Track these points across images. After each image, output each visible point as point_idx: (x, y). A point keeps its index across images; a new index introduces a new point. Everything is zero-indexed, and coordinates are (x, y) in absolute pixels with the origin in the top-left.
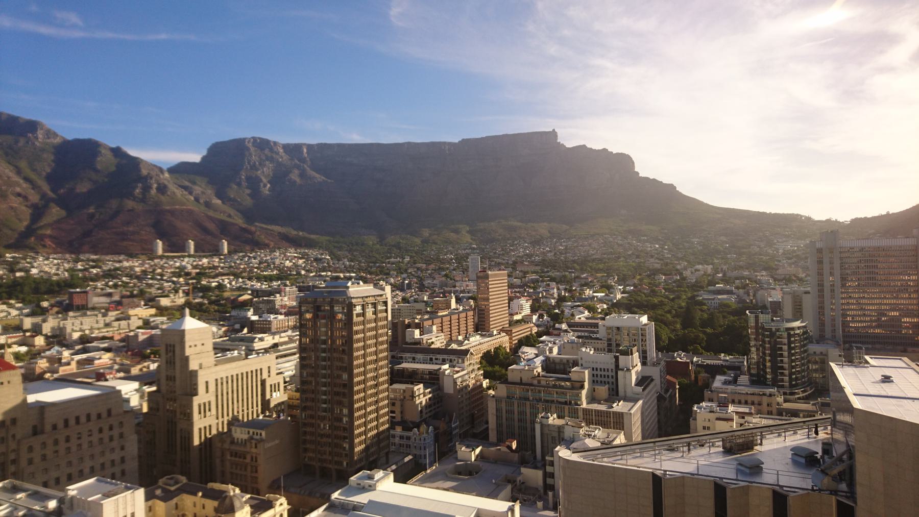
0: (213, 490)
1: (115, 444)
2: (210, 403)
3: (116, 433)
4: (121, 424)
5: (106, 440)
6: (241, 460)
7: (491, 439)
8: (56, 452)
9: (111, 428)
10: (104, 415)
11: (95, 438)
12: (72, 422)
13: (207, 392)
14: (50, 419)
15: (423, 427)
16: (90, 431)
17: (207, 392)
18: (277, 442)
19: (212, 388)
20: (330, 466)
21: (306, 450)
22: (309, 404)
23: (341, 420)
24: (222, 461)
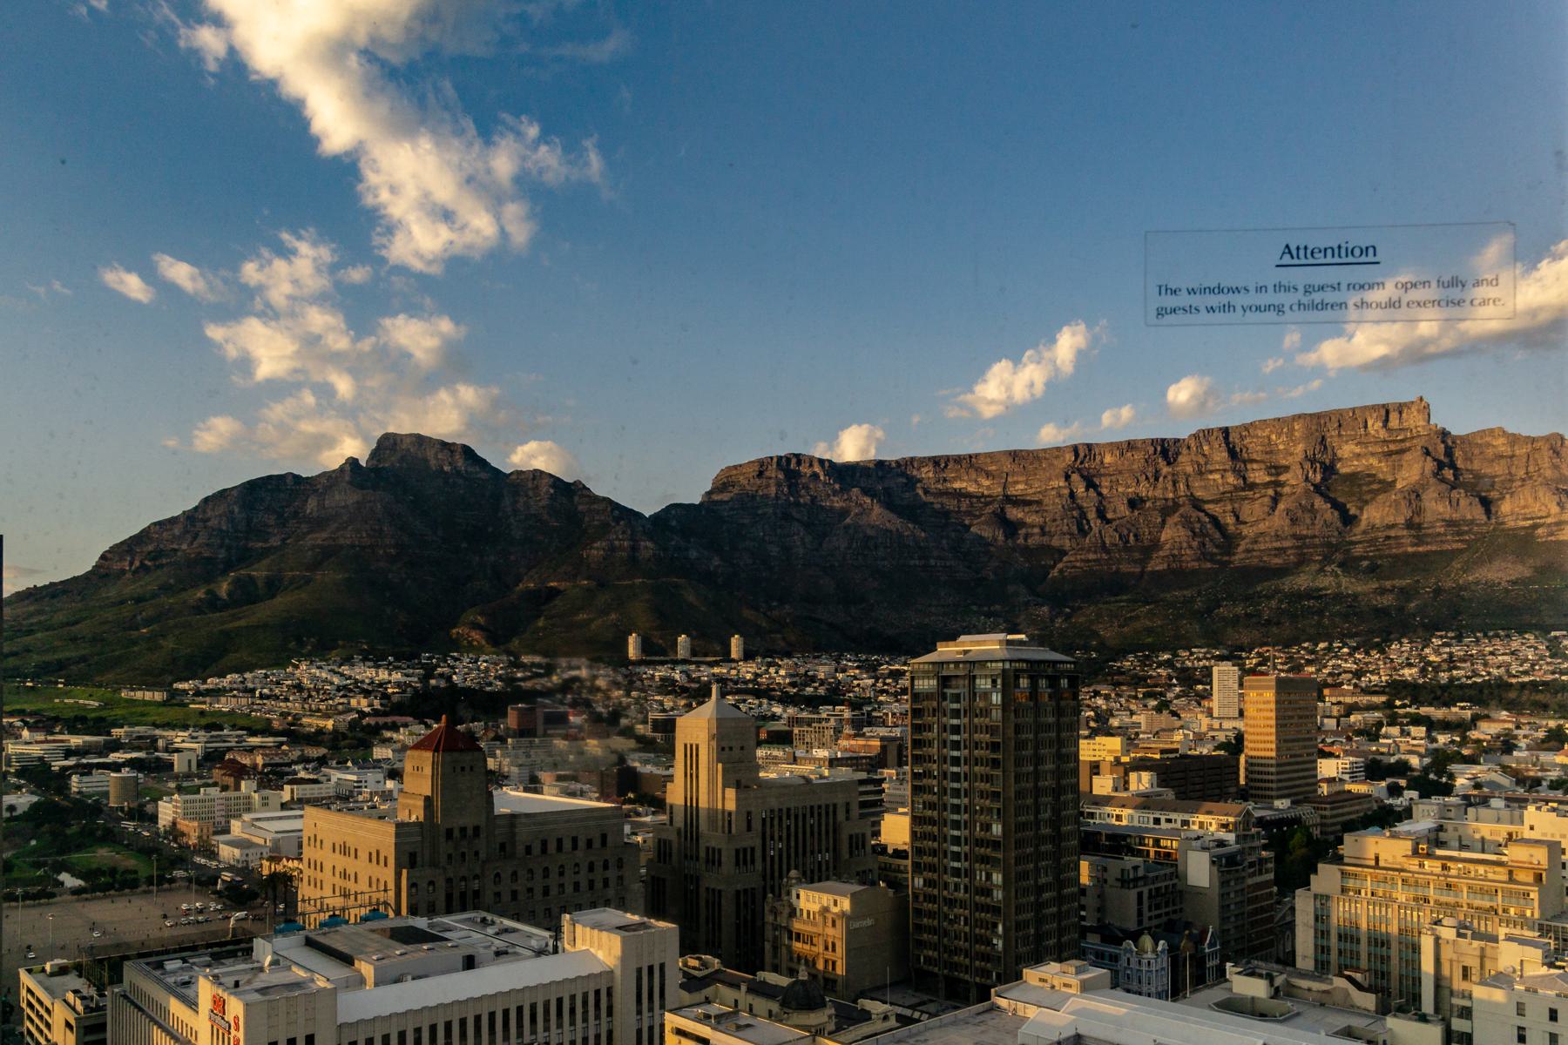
0: (764, 983)
1: (611, 892)
2: (753, 849)
3: (612, 874)
4: (620, 864)
5: (599, 885)
6: (807, 947)
7: (1300, 963)
8: (530, 890)
9: (606, 867)
10: (597, 844)
11: (583, 879)
12: (552, 847)
13: (749, 828)
14: (523, 834)
15: (1147, 941)
16: (577, 865)
17: (749, 828)
18: (869, 922)
19: (757, 825)
20: (967, 977)
21: (921, 944)
22: (927, 859)
23: (987, 892)
24: (775, 948)
